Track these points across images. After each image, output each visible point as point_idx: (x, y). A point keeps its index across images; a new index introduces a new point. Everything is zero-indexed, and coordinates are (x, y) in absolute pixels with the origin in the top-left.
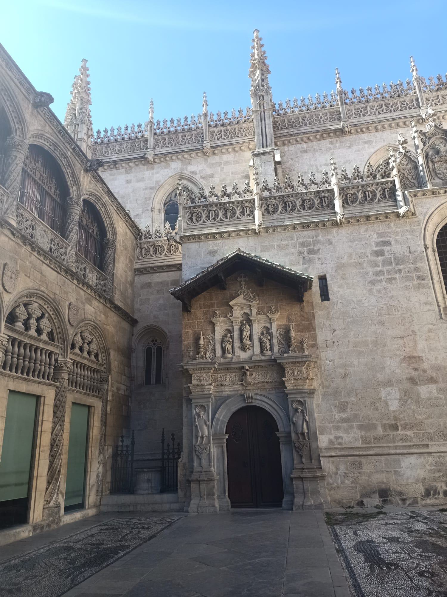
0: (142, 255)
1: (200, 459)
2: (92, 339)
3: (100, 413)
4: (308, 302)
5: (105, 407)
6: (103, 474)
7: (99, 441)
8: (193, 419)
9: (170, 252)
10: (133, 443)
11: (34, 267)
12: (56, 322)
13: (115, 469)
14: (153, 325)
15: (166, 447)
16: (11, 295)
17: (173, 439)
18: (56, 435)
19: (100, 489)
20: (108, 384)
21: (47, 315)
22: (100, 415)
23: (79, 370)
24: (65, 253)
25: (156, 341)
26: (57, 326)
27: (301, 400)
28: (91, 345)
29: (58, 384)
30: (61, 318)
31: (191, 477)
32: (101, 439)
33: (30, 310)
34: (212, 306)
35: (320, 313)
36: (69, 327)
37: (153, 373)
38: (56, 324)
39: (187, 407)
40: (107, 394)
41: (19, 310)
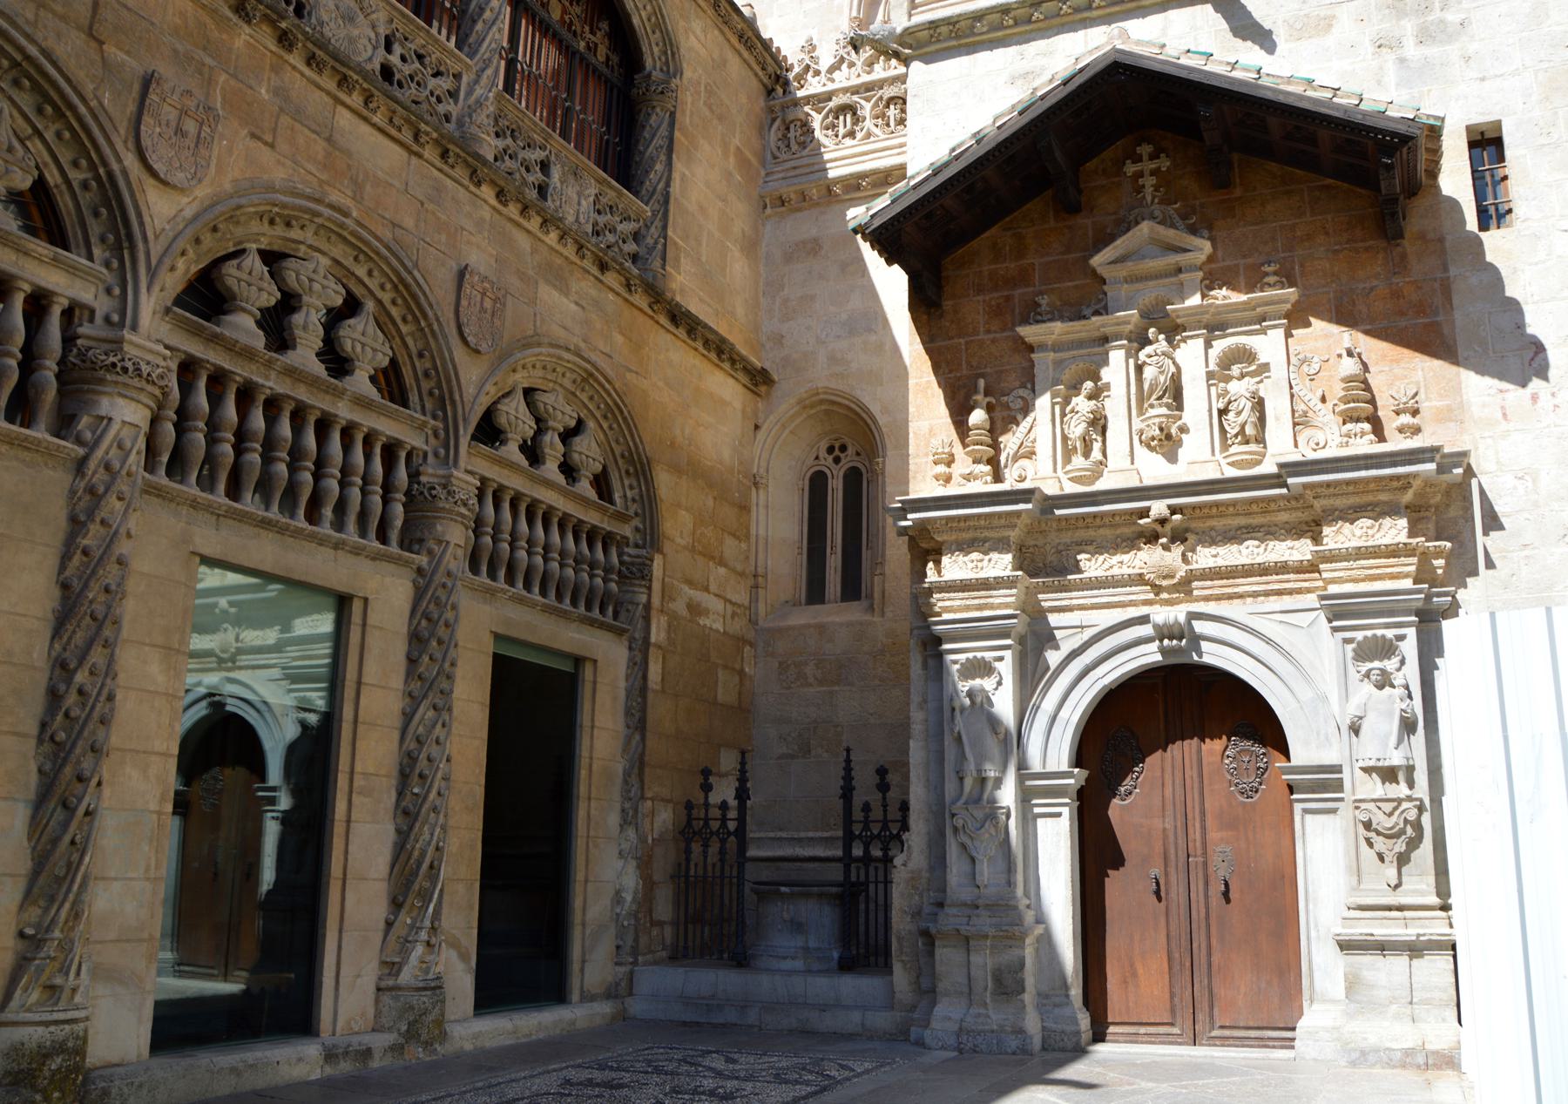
0: (788, 146)
1: (973, 860)
2: (580, 422)
3: (622, 684)
4: (1422, 236)
5: (639, 666)
6: (635, 893)
7: (619, 781)
8: (947, 714)
9: (888, 125)
10: (742, 794)
11: (298, 114)
12: (412, 334)
13: (683, 878)
14: (827, 391)
15: (858, 815)
16: (186, 200)
17: (883, 787)
18: (418, 741)
19: (630, 942)
20: (649, 588)
21: (370, 305)
22: (622, 694)
23: (523, 526)
24: (453, 94)
25: (843, 448)
26: (414, 351)
27: (1390, 634)
28: (577, 440)
29: (422, 560)
30: (425, 316)
31: (936, 921)
32: (627, 774)
33: (291, 279)
34: (1023, 278)
35: (1474, 281)
36: (459, 353)
37: (834, 562)
38: (410, 341)
39: (925, 666)
40: (647, 619)
41: (239, 267)
